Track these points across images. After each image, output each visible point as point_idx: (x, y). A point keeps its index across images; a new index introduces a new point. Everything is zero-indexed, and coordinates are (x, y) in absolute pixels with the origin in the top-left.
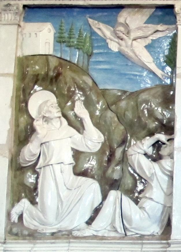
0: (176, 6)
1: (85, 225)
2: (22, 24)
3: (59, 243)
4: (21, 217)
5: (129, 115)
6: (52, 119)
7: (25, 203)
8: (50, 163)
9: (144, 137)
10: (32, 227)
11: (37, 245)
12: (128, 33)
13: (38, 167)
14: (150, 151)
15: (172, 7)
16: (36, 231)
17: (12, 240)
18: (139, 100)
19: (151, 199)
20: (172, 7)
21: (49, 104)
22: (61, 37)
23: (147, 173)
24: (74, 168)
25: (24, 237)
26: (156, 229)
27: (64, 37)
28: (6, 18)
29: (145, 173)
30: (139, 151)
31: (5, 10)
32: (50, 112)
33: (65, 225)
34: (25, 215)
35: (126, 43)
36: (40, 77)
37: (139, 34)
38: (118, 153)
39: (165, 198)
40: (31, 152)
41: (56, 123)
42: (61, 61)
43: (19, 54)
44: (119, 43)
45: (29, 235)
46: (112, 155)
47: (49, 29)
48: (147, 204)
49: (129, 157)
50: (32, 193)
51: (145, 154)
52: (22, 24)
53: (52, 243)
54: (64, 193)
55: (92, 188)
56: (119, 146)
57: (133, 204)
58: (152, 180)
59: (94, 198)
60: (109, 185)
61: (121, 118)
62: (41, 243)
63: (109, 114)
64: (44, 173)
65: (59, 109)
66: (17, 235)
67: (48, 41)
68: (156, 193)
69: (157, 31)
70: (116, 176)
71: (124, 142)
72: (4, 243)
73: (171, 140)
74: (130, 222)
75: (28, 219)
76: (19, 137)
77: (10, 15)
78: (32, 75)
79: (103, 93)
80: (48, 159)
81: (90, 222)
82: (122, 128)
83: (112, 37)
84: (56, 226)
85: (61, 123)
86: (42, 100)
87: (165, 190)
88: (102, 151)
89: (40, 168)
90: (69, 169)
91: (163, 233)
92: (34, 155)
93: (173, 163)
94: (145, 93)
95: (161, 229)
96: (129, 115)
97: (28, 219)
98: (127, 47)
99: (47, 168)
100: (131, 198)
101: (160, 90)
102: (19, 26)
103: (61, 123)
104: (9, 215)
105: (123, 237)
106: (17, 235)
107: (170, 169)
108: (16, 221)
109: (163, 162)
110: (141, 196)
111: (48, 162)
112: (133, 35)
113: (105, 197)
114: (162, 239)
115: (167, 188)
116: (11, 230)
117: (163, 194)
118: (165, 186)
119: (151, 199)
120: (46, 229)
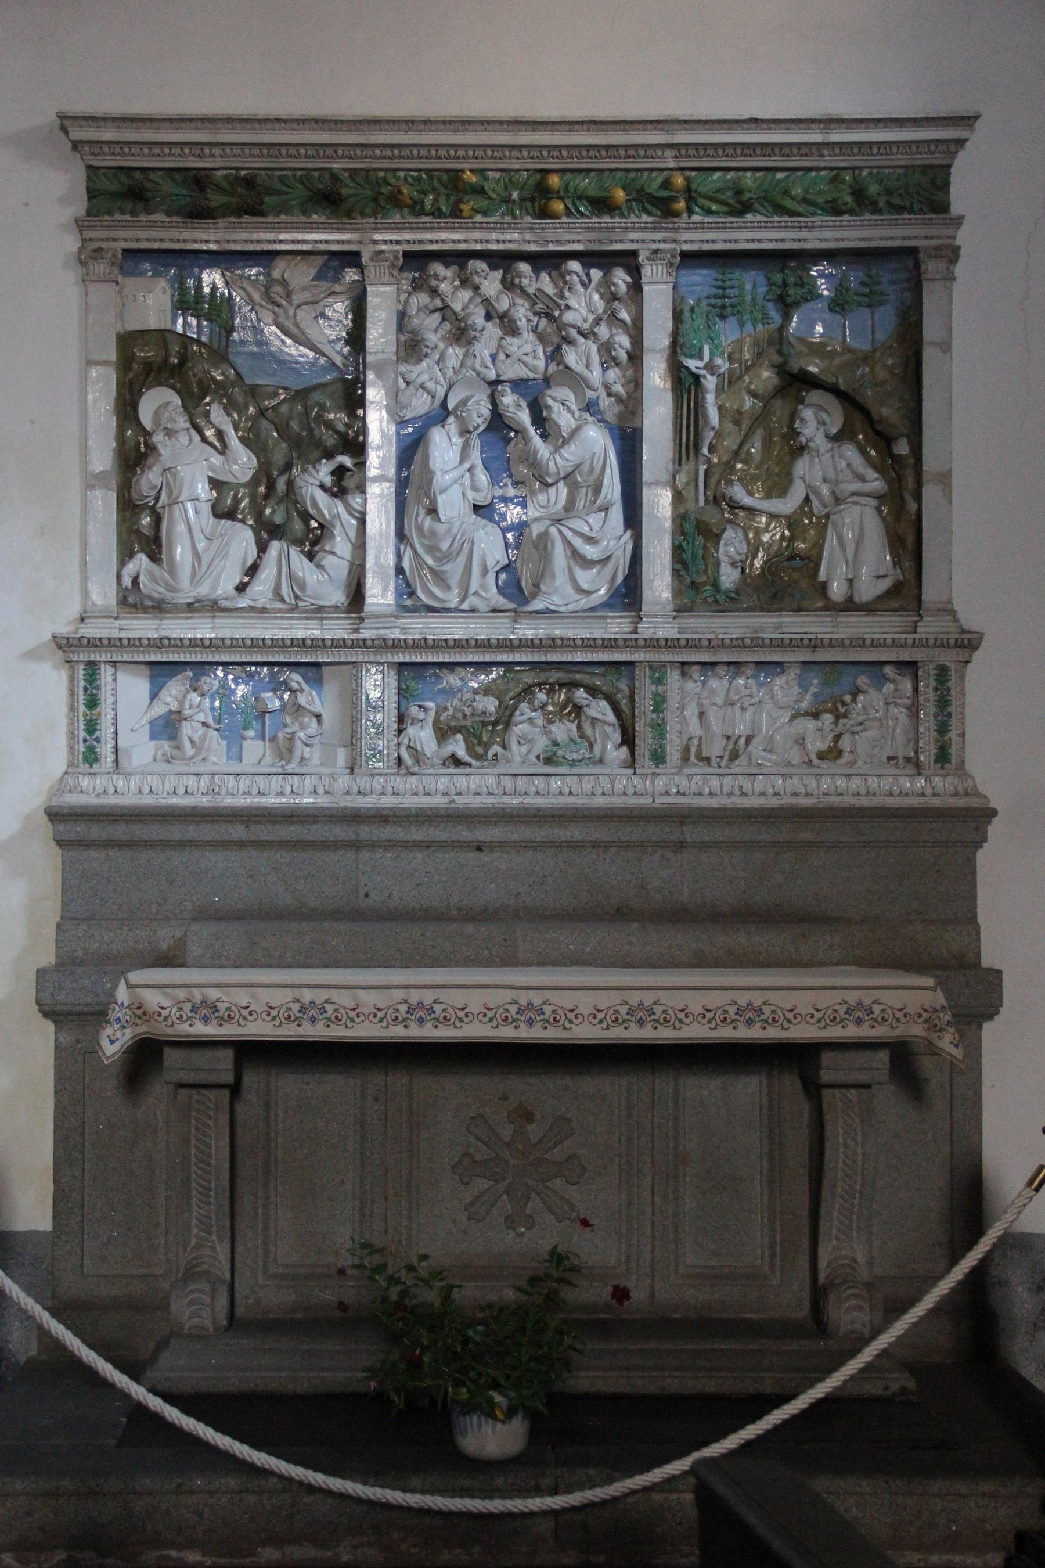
0: (363, 254)
1: (233, 592)
2: (120, 279)
3: (198, 618)
4: (135, 581)
5: (295, 425)
6: (177, 432)
7: (141, 561)
8: (180, 500)
9: (319, 460)
10: (156, 595)
11: (165, 622)
12: (288, 295)
13: (159, 505)
14: (328, 480)
15: (357, 255)
16: (163, 601)
17: (127, 613)
18: (309, 403)
19: (333, 553)
20: (357, 255)
21: (170, 408)
22: (184, 302)
23: (326, 513)
24: (213, 507)
25: (145, 610)
26: (339, 597)
27: (188, 302)
28: (97, 271)
29: (323, 515)
30: (312, 481)
31: (92, 258)
32: (175, 421)
33: (204, 590)
34: (142, 578)
35: (286, 312)
36: (155, 366)
37: (306, 296)
38: (281, 485)
39: (353, 552)
40: (150, 482)
41: (184, 439)
42: (185, 339)
43: (119, 328)
44: (274, 313)
45: (153, 607)
46: (271, 487)
47: (164, 288)
48: (328, 561)
49: (297, 491)
50: (154, 546)
51: (322, 487)
52: (120, 279)
53: (187, 618)
54: (201, 546)
55: (242, 540)
56: (281, 473)
57: (305, 560)
58: (333, 526)
59: (246, 554)
60: (268, 531)
61: (283, 431)
62: (171, 618)
63: (264, 424)
64: (171, 515)
65: (186, 418)
66: (134, 606)
67: (163, 308)
68: (341, 545)
69: (334, 292)
70: (278, 519)
71: (288, 467)
72: (116, 618)
73: (361, 465)
74: (303, 586)
75: (149, 584)
76: (126, 464)
77: (102, 266)
78: (144, 364)
79: (254, 392)
80: (175, 493)
81: (241, 588)
82: (284, 445)
83: (264, 303)
84: (192, 594)
85: (191, 440)
86: (157, 403)
87: (353, 540)
88: (255, 482)
89: (164, 507)
90: (206, 508)
91: (350, 604)
92: (154, 487)
93: (366, 500)
94: (319, 392)
95: (347, 597)
96: (295, 425)
97: (149, 584)
98: (287, 318)
99: (176, 507)
100: (302, 552)
101: (339, 386)
102: (117, 283)
103: (191, 440)
104: (119, 577)
105: (293, 609)
106: (134, 606)
107: (360, 508)
108: (130, 586)
109: (349, 498)
110: (316, 548)
111: (179, 496)
112: (297, 299)
113: (262, 548)
114: (349, 612)
115: (357, 538)
116: (125, 598)
117: (349, 546)
118: (353, 534)
119: (333, 553)
120: (178, 598)
